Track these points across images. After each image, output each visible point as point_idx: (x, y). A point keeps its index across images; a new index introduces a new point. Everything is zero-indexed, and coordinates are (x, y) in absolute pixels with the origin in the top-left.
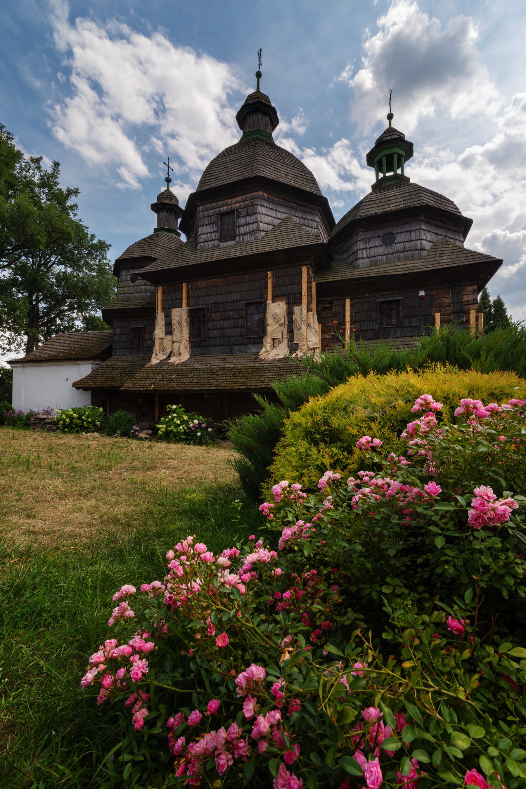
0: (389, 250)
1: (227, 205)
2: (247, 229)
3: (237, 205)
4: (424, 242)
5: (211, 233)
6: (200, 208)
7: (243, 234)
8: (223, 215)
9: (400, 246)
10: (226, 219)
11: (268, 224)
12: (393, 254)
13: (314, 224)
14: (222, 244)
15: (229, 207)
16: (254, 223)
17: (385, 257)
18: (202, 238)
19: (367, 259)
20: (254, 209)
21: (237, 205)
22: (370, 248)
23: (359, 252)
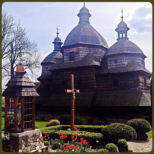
0: (116, 64)
1: (72, 50)
2: (77, 57)
3: (74, 50)
4: (125, 62)
5: (67, 58)
6: (64, 50)
7: (76, 59)
8: (70, 53)
9: (118, 63)
10: (71, 54)
11: (83, 56)
12: (117, 65)
13: (98, 53)
14: (70, 62)
15: (72, 51)
16: (79, 56)
17: (115, 66)
18: (65, 59)
19: (110, 67)
20: (79, 52)
21: (74, 50)
22: (111, 63)
23: (108, 64)
